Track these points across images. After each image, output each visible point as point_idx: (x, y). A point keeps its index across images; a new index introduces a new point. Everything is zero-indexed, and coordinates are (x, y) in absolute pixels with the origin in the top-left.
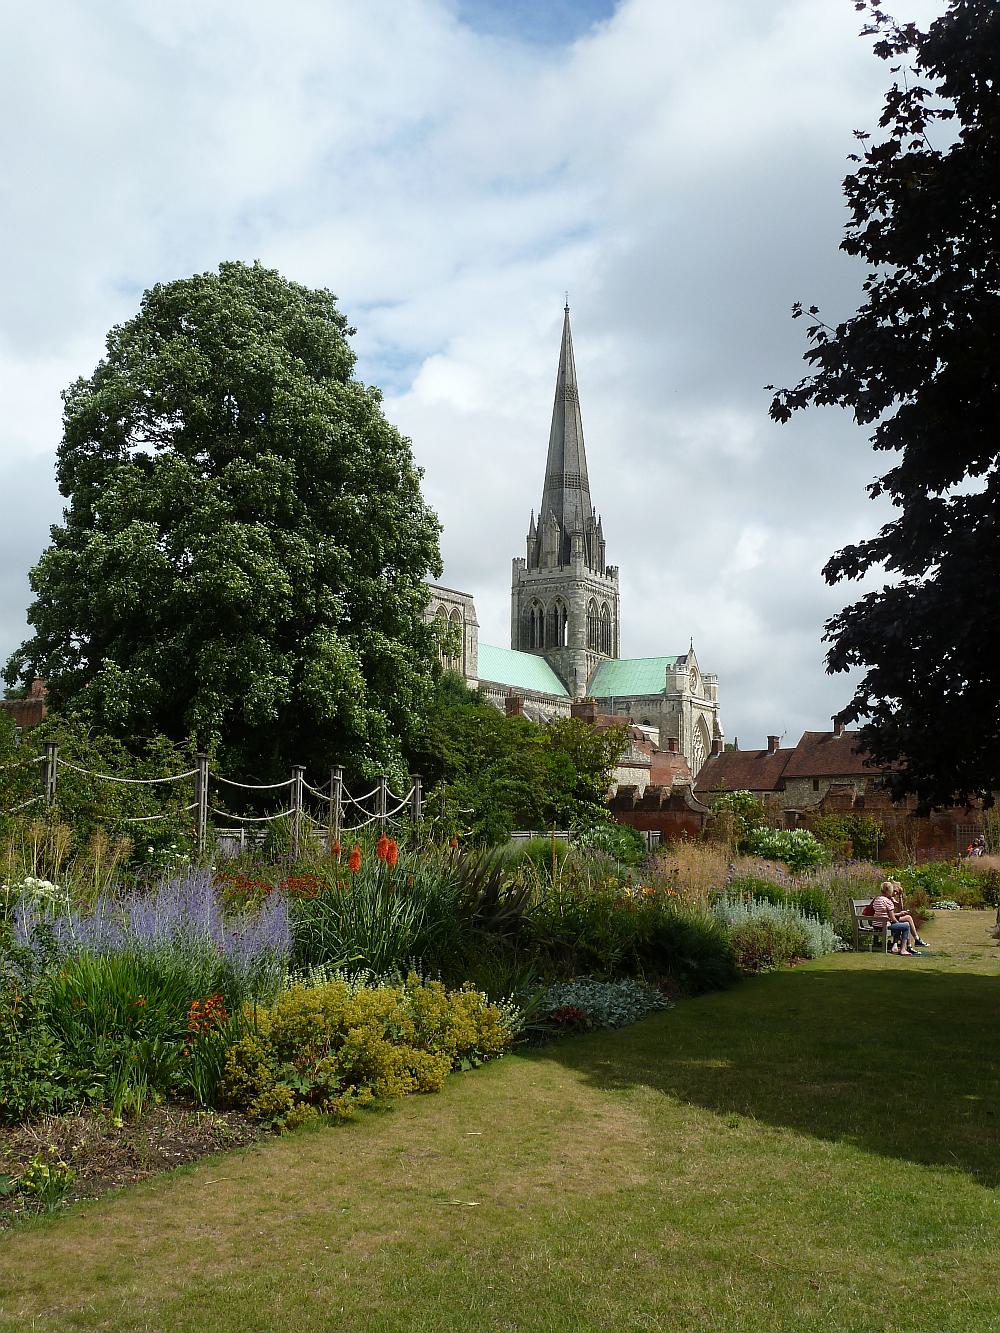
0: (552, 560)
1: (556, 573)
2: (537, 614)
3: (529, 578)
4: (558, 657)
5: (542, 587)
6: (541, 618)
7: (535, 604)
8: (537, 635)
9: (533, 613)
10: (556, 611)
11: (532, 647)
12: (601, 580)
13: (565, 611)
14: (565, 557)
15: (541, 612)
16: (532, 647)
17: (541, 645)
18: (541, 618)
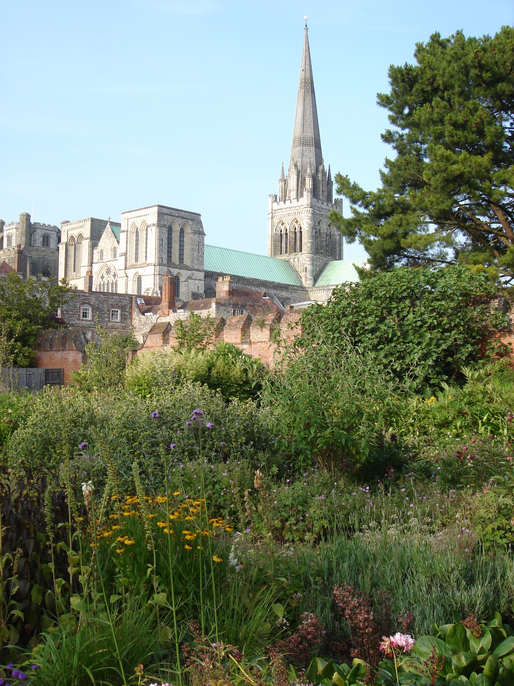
0: (293, 195)
1: (295, 203)
2: (283, 232)
3: (278, 207)
4: (296, 260)
5: (286, 213)
6: (286, 234)
7: (283, 224)
8: (284, 245)
9: (281, 231)
10: (295, 229)
11: (281, 253)
12: (327, 208)
13: (301, 228)
14: (299, 195)
15: (286, 230)
16: (281, 253)
17: (286, 252)
18: (286, 234)
